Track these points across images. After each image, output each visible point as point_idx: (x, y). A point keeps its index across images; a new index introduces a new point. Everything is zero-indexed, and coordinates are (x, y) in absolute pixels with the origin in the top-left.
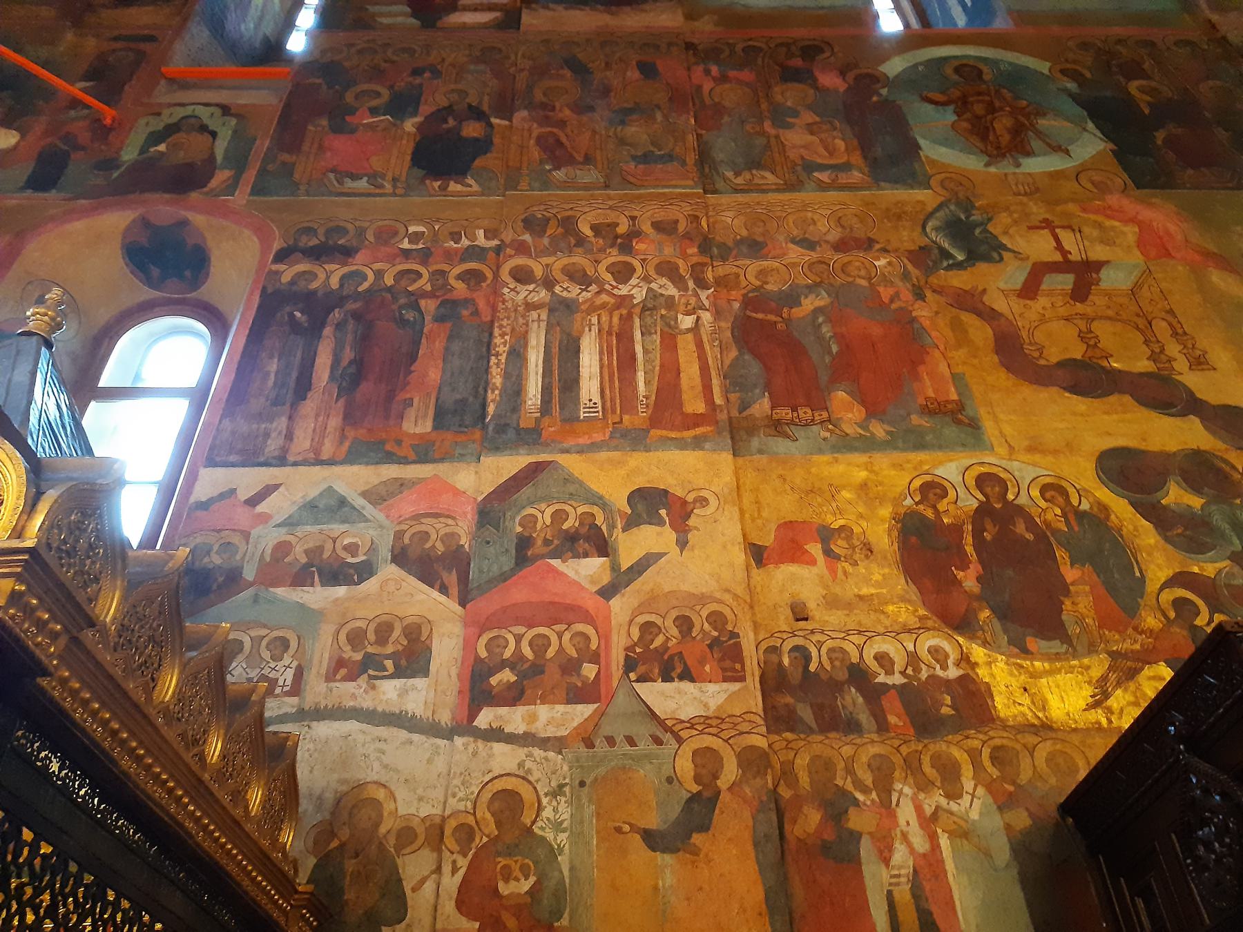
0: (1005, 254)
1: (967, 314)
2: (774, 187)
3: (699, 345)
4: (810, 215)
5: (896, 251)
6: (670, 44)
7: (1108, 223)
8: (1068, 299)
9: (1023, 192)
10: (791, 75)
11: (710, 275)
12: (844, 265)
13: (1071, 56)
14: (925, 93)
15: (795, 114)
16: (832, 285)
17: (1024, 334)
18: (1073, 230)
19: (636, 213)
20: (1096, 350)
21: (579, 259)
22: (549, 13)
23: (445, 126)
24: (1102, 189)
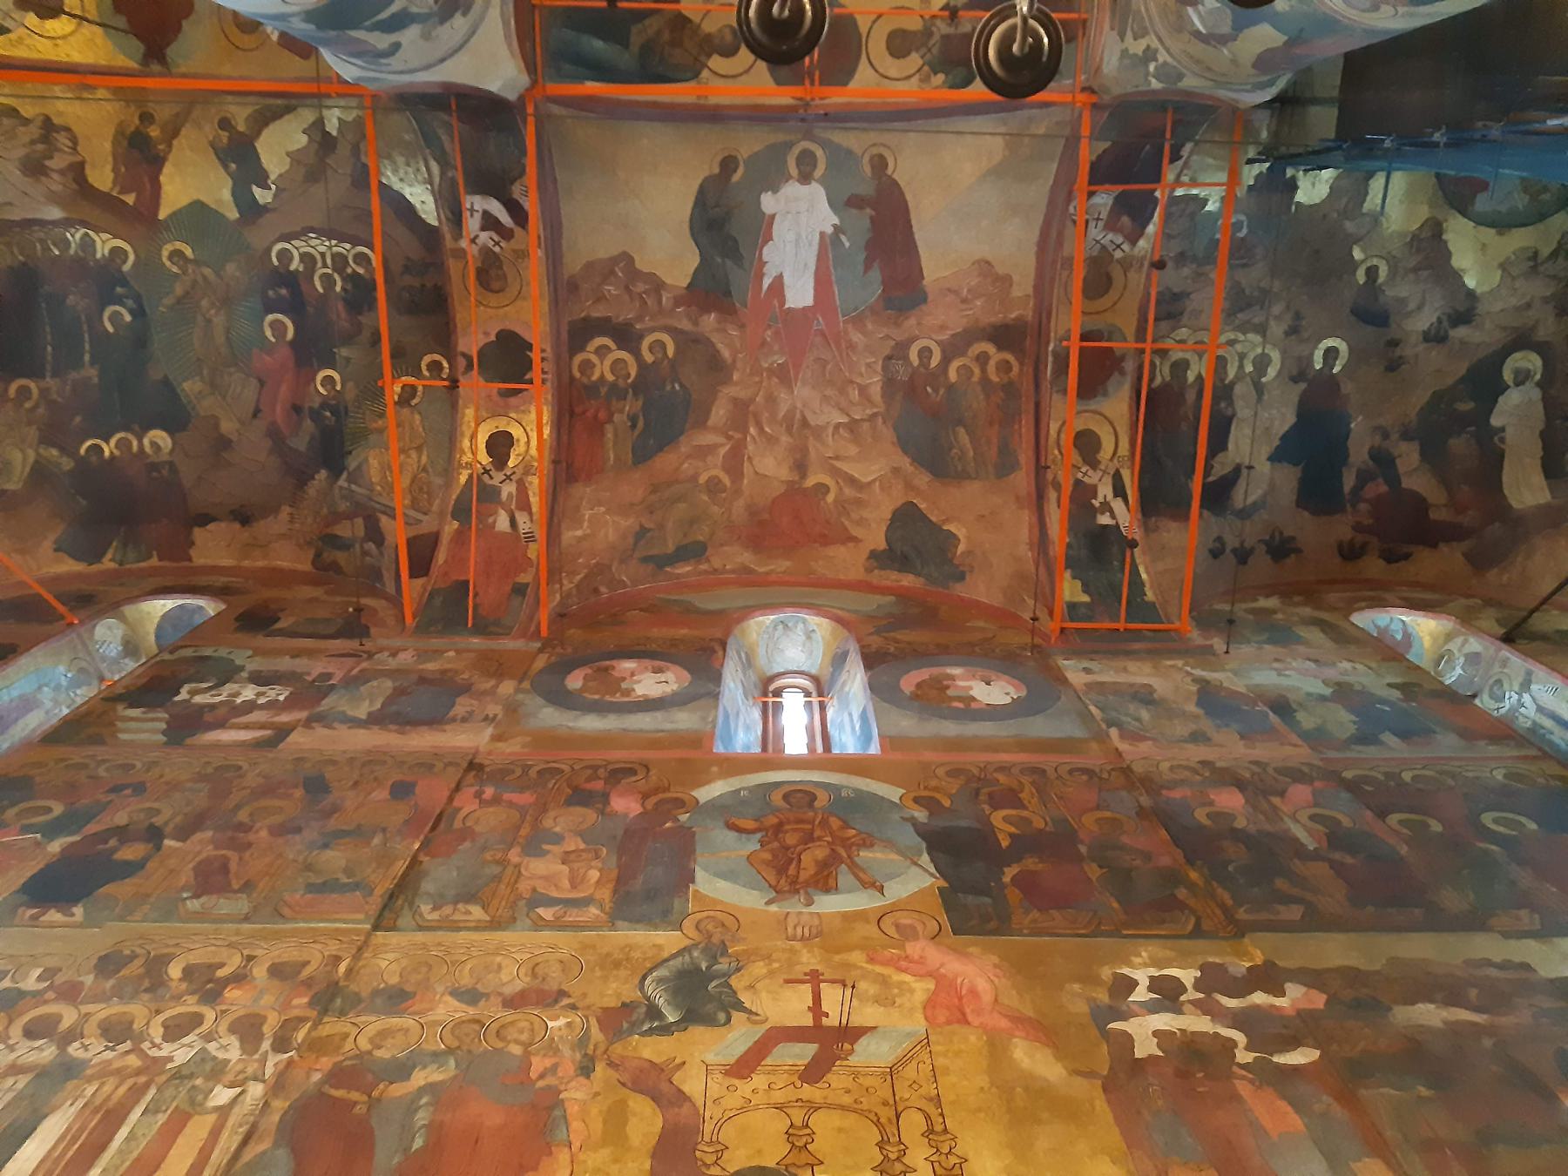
0: (737, 1016)
1: (640, 1097)
2: (473, 924)
3: (215, 1133)
4: (499, 959)
5: (588, 1007)
6: (447, 765)
7: (898, 977)
8: (795, 1078)
9: (799, 937)
10: (580, 797)
11: (300, 1036)
12: (502, 1026)
13: (933, 783)
14: (733, 820)
15: (558, 839)
16: (469, 1052)
17: (708, 1128)
18: (845, 986)
19: (259, 952)
20: (804, 1153)
21: (137, 1010)
22: (326, 731)
23: (101, 847)
24: (908, 934)
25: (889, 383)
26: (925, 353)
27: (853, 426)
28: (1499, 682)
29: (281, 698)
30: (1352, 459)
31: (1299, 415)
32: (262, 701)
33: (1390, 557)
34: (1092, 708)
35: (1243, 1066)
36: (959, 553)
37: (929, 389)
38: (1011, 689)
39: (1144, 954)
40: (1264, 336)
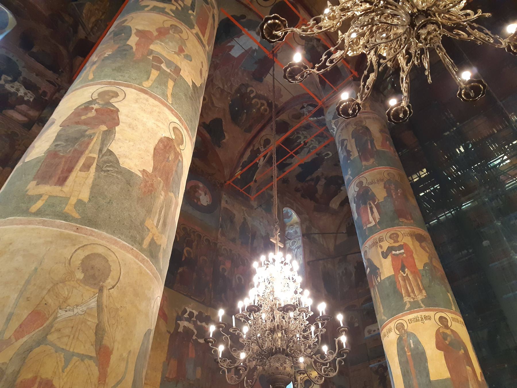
25: (238, 90)
26: (252, 92)
27: (222, 91)
28: (295, 242)
29: (31, 100)
30: (313, 175)
31: (311, 161)
32: (26, 99)
33: (303, 196)
34: (221, 218)
35: (193, 340)
36: (223, 141)
37: (246, 99)
38: (208, 200)
39: (192, 304)
40: (319, 144)
